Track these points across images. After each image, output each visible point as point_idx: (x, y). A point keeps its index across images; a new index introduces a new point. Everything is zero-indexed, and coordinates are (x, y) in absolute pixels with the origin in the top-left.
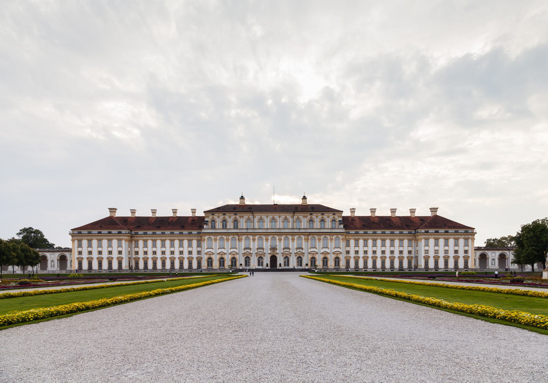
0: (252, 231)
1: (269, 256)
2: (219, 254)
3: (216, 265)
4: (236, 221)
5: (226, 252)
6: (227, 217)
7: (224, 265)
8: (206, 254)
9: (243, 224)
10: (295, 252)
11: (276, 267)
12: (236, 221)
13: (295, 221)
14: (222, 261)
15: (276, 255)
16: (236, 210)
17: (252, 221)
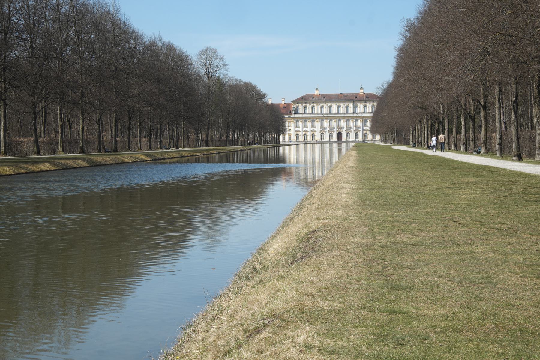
0: (325, 115)
1: (337, 132)
2: (304, 131)
3: (301, 138)
4: (313, 107)
5: (308, 130)
6: (308, 105)
7: (307, 139)
8: (296, 131)
9: (317, 109)
10: (355, 129)
11: (341, 140)
12: (313, 107)
13: (354, 107)
14: (305, 136)
15: (342, 132)
16: (314, 99)
17: (325, 107)
